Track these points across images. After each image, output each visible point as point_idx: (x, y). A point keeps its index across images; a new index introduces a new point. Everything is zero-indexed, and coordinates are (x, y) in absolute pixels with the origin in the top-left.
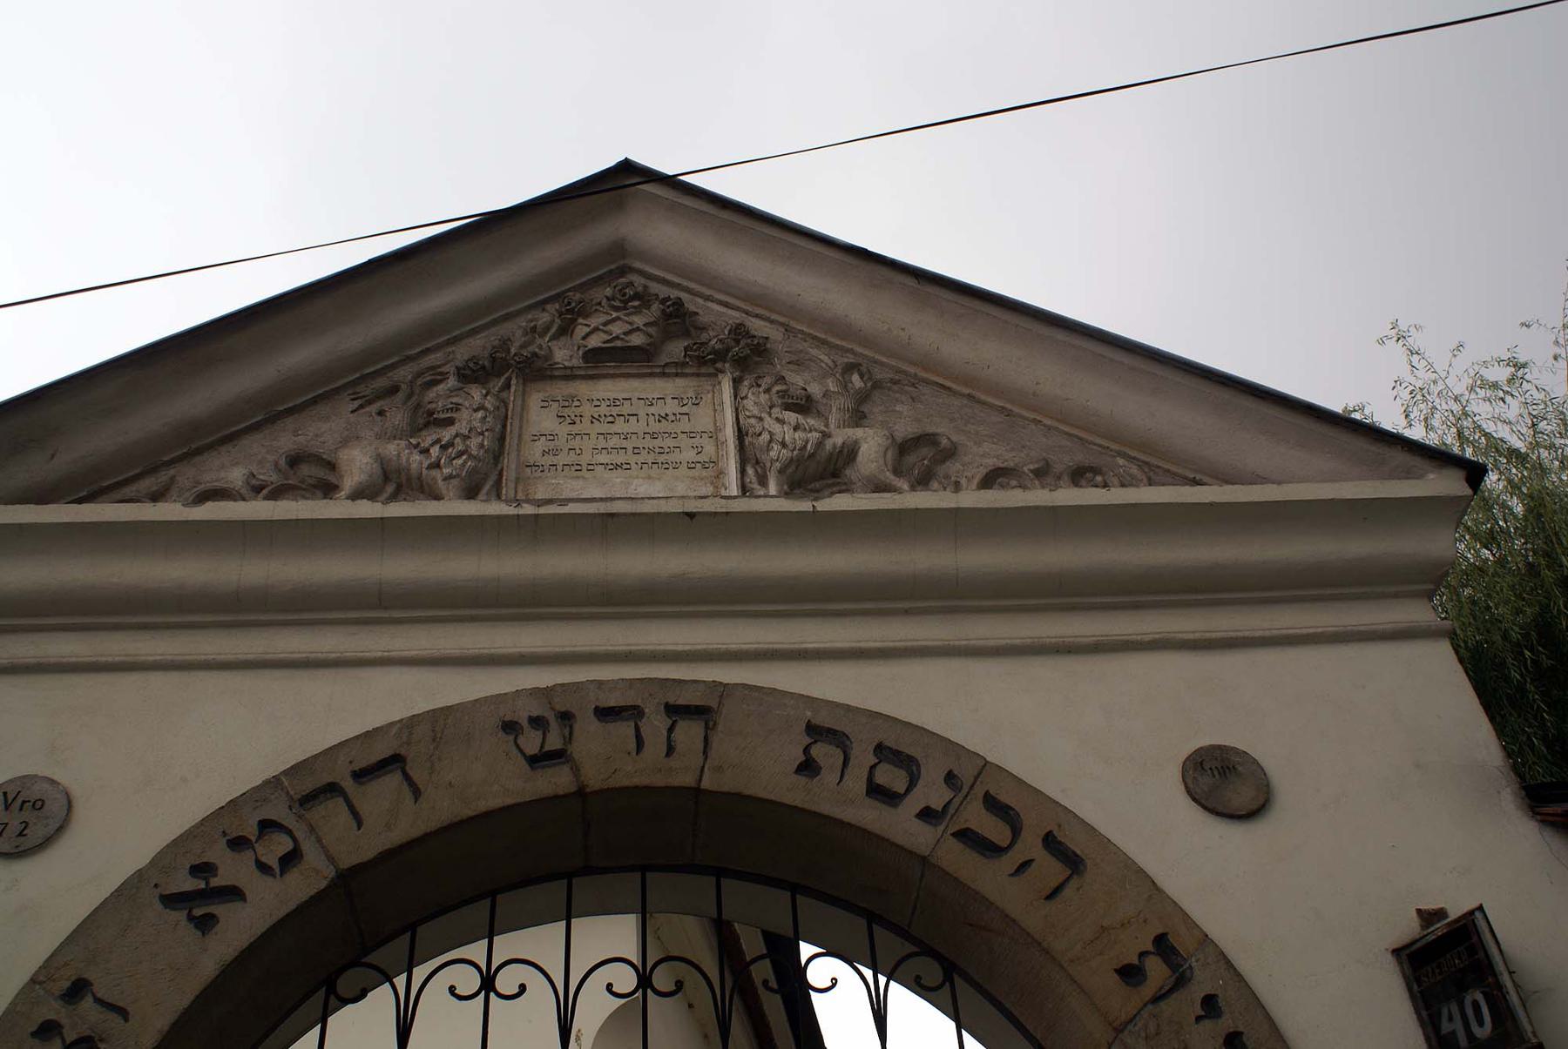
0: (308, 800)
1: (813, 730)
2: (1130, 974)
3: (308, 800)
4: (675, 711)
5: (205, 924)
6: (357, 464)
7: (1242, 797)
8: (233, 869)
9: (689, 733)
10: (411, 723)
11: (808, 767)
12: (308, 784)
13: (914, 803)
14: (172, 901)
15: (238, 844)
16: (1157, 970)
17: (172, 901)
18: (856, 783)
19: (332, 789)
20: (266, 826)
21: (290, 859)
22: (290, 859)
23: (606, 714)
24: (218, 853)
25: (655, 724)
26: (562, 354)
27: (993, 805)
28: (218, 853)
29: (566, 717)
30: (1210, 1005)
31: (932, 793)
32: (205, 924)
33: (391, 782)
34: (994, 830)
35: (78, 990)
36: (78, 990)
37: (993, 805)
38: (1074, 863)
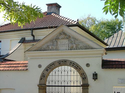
0: (50, 66)
1: (71, 62)
2: (82, 74)
3: (50, 66)
4: (65, 61)
5: (47, 71)
6: (50, 47)
7: (89, 66)
8: (48, 69)
9: (65, 62)
10: (54, 62)
11: (70, 64)
12: (51, 65)
13: (74, 66)
14: (46, 70)
15: (48, 68)
16: (83, 74)
17: (46, 70)
18: (72, 65)
19: (51, 65)
20: (49, 67)
21: (50, 68)
22: (50, 68)
23: (62, 61)
24: (47, 68)
25: (64, 62)
26: (60, 38)
27: (77, 66)
28: (47, 68)
29: (60, 62)
30: (84, 76)
31: (75, 66)
32: (47, 71)
33: (53, 65)
34: (77, 67)
35: (43, 74)
36: (43, 74)
37: (77, 66)
38: (80, 69)
